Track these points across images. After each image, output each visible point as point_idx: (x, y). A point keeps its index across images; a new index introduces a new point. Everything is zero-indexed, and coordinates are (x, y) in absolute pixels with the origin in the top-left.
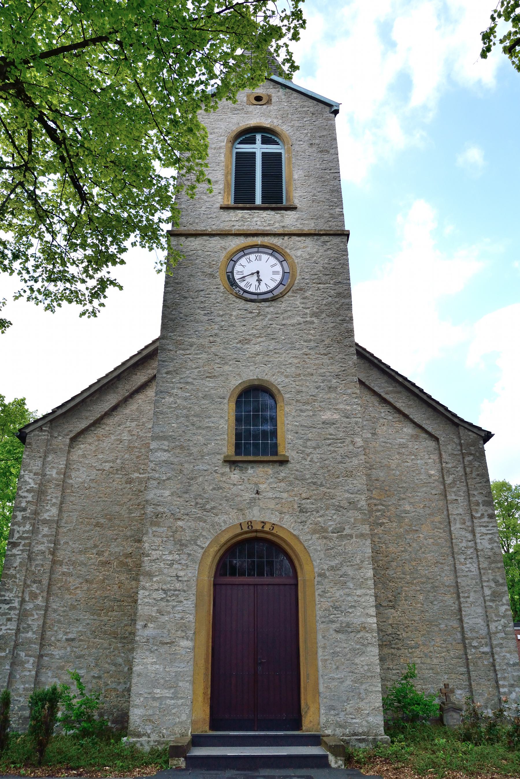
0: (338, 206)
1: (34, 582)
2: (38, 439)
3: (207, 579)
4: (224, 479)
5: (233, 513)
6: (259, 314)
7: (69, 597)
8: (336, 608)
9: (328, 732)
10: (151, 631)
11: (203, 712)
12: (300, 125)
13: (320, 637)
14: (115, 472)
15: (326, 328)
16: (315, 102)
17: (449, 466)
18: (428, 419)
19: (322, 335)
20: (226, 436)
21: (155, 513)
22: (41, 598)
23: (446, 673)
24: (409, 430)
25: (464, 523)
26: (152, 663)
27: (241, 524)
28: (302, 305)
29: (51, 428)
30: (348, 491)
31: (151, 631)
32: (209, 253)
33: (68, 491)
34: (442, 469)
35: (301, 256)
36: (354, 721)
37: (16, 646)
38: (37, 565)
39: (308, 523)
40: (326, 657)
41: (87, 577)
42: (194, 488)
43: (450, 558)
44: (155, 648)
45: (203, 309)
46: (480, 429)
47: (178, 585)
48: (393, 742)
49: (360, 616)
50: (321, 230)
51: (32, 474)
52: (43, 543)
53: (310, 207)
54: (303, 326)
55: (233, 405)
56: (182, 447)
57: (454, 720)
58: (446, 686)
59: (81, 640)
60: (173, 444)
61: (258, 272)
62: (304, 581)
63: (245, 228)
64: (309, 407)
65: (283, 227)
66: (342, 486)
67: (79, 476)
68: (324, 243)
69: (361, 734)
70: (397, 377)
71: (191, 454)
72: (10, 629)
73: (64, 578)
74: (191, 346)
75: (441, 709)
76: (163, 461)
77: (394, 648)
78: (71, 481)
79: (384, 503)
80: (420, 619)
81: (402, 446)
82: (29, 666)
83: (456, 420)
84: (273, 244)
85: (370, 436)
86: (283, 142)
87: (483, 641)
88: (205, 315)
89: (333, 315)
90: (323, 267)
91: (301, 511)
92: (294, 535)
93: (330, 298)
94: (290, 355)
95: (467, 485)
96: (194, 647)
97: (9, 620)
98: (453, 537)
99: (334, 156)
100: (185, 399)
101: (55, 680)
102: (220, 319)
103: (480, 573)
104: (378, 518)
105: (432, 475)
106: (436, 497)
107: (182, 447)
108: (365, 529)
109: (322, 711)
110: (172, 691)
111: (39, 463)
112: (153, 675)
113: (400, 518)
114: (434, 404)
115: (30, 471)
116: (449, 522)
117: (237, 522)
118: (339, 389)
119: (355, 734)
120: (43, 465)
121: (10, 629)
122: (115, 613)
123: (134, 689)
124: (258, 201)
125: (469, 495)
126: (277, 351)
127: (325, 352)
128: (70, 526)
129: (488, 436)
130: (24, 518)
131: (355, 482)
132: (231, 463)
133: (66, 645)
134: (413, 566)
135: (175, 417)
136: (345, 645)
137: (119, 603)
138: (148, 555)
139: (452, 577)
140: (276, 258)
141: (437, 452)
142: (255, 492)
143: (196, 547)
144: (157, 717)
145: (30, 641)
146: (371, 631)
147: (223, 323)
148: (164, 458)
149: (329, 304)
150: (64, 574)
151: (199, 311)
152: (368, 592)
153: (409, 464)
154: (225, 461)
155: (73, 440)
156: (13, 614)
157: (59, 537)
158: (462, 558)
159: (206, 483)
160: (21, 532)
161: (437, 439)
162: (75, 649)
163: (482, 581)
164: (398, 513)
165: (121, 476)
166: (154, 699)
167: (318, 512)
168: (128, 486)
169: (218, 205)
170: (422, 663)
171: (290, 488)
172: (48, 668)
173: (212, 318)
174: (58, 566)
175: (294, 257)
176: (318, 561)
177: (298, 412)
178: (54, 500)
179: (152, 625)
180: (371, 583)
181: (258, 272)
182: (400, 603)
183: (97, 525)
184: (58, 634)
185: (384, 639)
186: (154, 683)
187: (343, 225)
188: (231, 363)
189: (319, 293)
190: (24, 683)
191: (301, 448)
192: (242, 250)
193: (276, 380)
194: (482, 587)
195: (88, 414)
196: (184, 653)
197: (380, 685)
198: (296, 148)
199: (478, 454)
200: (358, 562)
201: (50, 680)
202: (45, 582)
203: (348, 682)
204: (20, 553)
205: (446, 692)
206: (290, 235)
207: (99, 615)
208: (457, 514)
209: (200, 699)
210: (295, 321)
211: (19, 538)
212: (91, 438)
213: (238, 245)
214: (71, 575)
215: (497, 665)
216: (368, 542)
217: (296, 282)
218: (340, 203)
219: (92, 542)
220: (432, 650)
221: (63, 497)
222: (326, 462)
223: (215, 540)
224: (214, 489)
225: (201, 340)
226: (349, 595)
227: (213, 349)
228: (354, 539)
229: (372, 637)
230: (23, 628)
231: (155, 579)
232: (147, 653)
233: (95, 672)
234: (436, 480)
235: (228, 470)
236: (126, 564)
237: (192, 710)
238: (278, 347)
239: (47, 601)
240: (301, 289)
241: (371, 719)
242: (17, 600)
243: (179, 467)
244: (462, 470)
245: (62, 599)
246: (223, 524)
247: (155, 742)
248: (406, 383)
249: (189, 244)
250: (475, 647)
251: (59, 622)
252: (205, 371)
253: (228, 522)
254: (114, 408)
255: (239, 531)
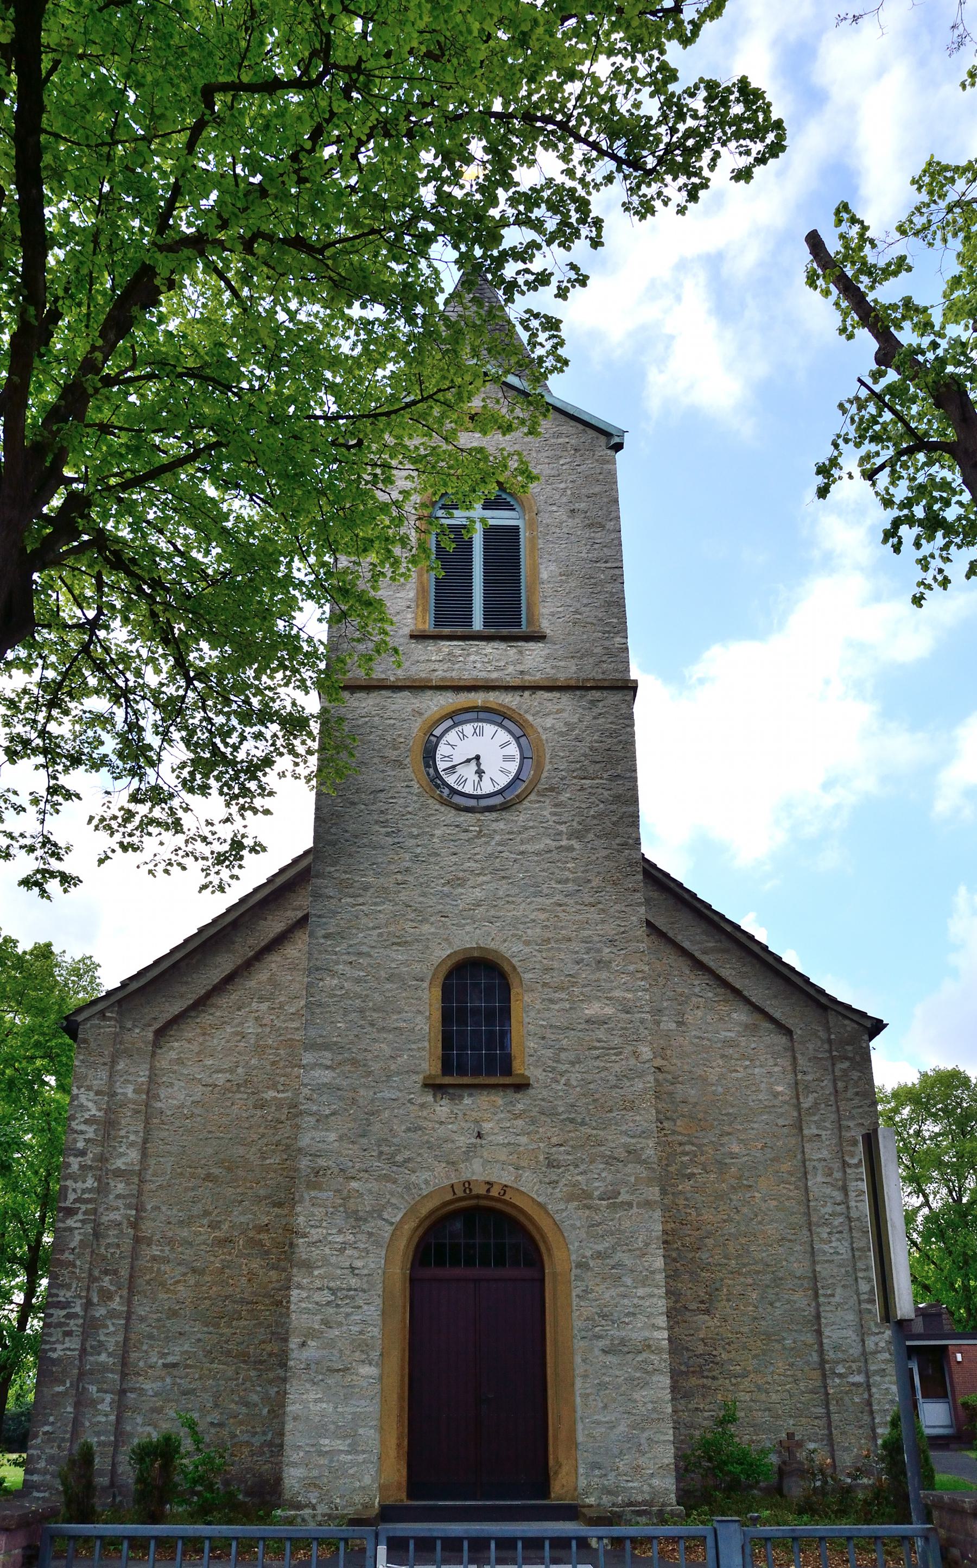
0: (618, 632)
1: (106, 1272)
2: (98, 1032)
3: (399, 1271)
4: (425, 1113)
5: (440, 1168)
6: (480, 834)
7: (166, 1296)
8: (604, 1316)
9: (591, 1500)
10: (313, 1351)
11: (396, 1472)
12: (553, 473)
13: (578, 1359)
14: (235, 1088)
15: (594, 858)
16: (581, 427)
17: (809, 1078)
18: (775, 997)
19: (587, 871)
20: (426, 1044)
21: (313, 1168)
22: (118, 1299)
23: (791, 1416)
24: (741, 1016)
25: (830, 1175)
26: (316, 1401)
27: (452, 1186)
28: (554, 818)
29: (120, 1013)
30: (625, 1133)
31: (313, 1351)
32: (392, 722)
33: (155, 1121)
34: (797, 1084)
35: (553, 727)
36: (630, 1484)
37: (81, 1375)
38: (108, 1246)
39: (561, 1184)
40: (588, 1391)
41: (194, 1264)
42: (376, 1127)
43: (805, 1232)
44: (320, 1377)
45: (384, 824)
46: (863, 1014)
47: (353, 1282)
48: (688, 1515)
49: (641, 1329)
50: (588, 680)
51: (92, 1094)
52: (118, 1209)
53: (569, 634)
54: (555, 856)
55: (437, 992)
56: (354, 1062)
57: (796, 1489)
58: (790, 1436)
59: (187, 1366)
60: (340, 1057)
61: (478, 758)
62: (554, 1274)
63: (454, 674)
64: (563, 996)
65: (522, 672)
66: (616, 1124)
67: (174, 1096)
68: (593, 703)
69: (640, 1504)
70: (723, 924)
71: (370, 1073)
72: (69, 1349)
73: (156, 1266)
74: (366, 889)
75: (781, 1472)
76: (325, 1085)
77: (707, 1377)
78: (159, 1105)
79: (695, 1141)
80: (752, 1331)
81: (728, 1043)
82: (105, 1407)
83: (823, 1000)
84: (504, 706)
85: (673, 1026)
86: (522, 505)
87: (854, 1366)
88: (388, 834)
89: (607, 835)
90: (591, 749)
91: (550, 1165)
92: (539, 1204)
93: (602, 806)
94: (533, 906)
95: (838, 1111)
96: (381, 1378)
97: (68, 1334)
98: (811, 1198)
99: (613, 536)
100: (358, 981)
101: (149, 1429)
102: (412, 842)
103: (854, 1256)
104: (684, 1165)
105: (778, 1093)
106: (785, 1130)
107: (354, 1062)
108: (653, 1193)
109: (581, 1471)
110: (349, 1441)
111: (104, 1074)
112: (317, 1419)
113: (722, 1167)
114: (786, 972)
115: (89, 1088)
116: (806, 1173)
117: (447, 1182)
118: (614, 964)
119: (631, 1504)
120: (111, 1076)
121: (69, 1349)
122: (243, 1323)
123: (288, 1439)
124: (478, 623)
125: (840, 1127)
126: (510, 899)
127: (592, 900)
128: (160, 1181)
129: (877, 1026)
130: (82, 1167)
131: (638, 1118)
132: (435, 1088)
133: (163, 1373)
134: (741, 1244)
135: (341, 1011)
136: (618, 1373)
137: (249, 1307)
138: (305, 1236)
139: (807, 1263)
140: (510, 732)
141: (789, 1054)
142: (475, 1134)
143: (380, 1223)
144: (326, 1480)
145: (104, 1368)
146: (659, 1351)
147: (419, 850)
148: (325, 1080)
149: (600, 815)
150: (154, 1259)
151: (377, 828)
152: (656, 1291)
153: (739, 1075)
154: (426, 1085)
155: (161, 1033)
156: (73, 1324)
157: (143, 1198)
158: (824, 1232)
159: (395, 1121)
160: (79, 1192)
161: (789, 1032)
162: (178, 1380)
163: (855, 1270)
164: (718, 1158)
165: (245, 1096)
166: (321, 1454)
167: (577, 1166)
168: (259, 1113)
169: (406, 631)
170: (752, 1400)
171: (532, 1128)
172: (136, 1410)
173: (400, 840)
174: (144, 1247)
175: (540, 730)
176: (577, 1244)
177: (546, 1003)
178: (132, 1137)
179: (314, 1344)
180: (660, 1277)
181: (478, 758)
182: (719, 1305)
183: (209, 1177)
184: (151, 1357)
185: (691, 1362)
186: (321, 1430)
187: (627, 670)
188: (432, 919)
189: (583, 795)
190: (98, 1434)
191: (550, 1063)
192: (450, 716)
193: (510, 948)
194: (856, 1279)
195: (184, 989)
196: (365, 1384)
197: (671, 1432)
198: (545, 518)
199: (858, 1058)
200: (641, 1245)
201: (140, 1429)
202: (124, 1273)
203: (622, 1428)
204: (79, 1225)
205: (790, 1445)
206: (535, 688)
207: (217, 1326)
208: (820, 1160)
209: (393, 1453)
210: (542, 846)
211: (75, 1201)
212: (190, 1031)
213: (442, 707)
214: (166, 1260)
215: (874, 1402)
216: (657, 1214)
217: (545, 774)
218: (621, 628)
219: (200, 1205)
220: (769, 1379)
221: (147, 1131)
222: (591, 1086)
223: (412, 1210)
224: (409, 1130)
225: (382, 880)
226: (625, 1296)
227: (403, 896)
228: (635, 1210)
229: (661, 1360)
230: (92, 1347)
231: (316, 1273)
232: (308, 1386)
233: (215, 1417)
234: (785, 1102)
235: (430, 1098)
236: (260, 1243)
237: (379, 1471)
238: (512, 892)
239: (129, 1303)
240: (552, 789)
241: (656, 1482)
242: (79, 1302)
243: (351, 1094)
244: (830, 1085)
245: (154, 1300)
246: (423, 1186)
247: (324, 1515)
248: (738, 935)
249: (356, 704)
250: (840, 1376)
251: (151, 1337)
252: (389, 933)
253: (432, 1181)
254: (229, 979)
255: (449, 1197)
